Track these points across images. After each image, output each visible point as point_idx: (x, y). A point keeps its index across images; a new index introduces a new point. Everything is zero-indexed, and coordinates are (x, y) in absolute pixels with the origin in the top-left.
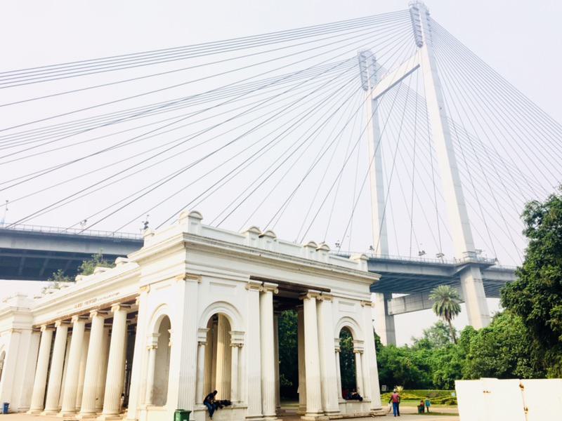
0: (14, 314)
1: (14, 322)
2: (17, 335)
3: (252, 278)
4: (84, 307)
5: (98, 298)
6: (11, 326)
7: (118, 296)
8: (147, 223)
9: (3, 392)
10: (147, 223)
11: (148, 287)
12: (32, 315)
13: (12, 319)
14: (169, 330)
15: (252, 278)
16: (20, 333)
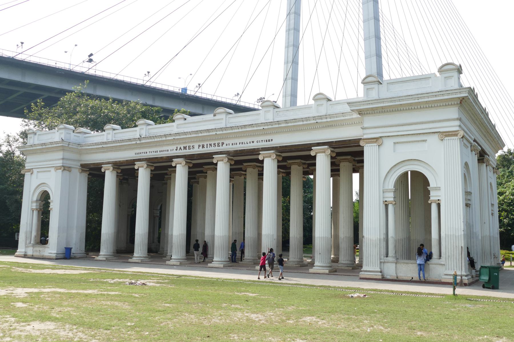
0: (63, 150)
1: (63, 159)
2: (66, 173)
3: (475, 141)
4: (197, 150)
5: (226, 142)
6: (60, 163)
7: (271, 143)
8: (91, 55)
9: (59, 236)
10: (91, 55)
11: (380, 141)
12: (80, 152)
13: (60, 155)
14: (428, 187)
15: (475, 141)
16: (70, 171)
